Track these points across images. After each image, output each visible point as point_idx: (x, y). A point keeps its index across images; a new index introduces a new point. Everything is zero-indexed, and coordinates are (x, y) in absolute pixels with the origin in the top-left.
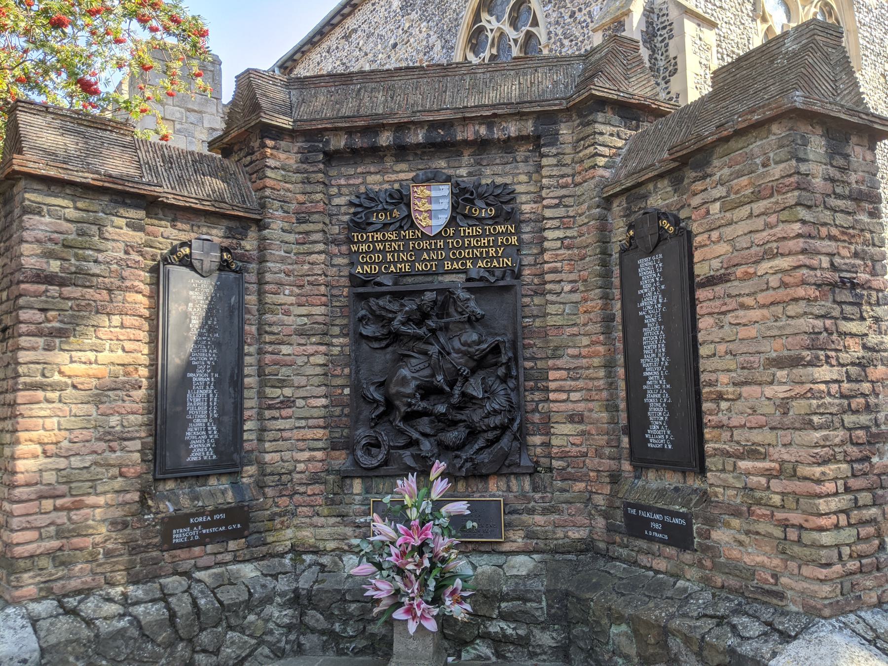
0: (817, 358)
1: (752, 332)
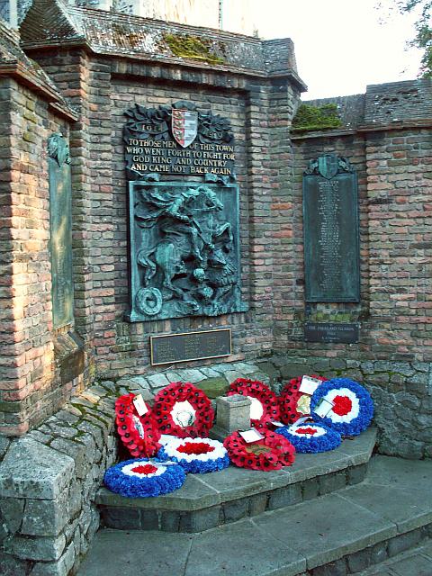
1: (405, 230)
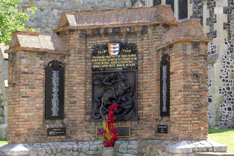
0: (185, 90)
